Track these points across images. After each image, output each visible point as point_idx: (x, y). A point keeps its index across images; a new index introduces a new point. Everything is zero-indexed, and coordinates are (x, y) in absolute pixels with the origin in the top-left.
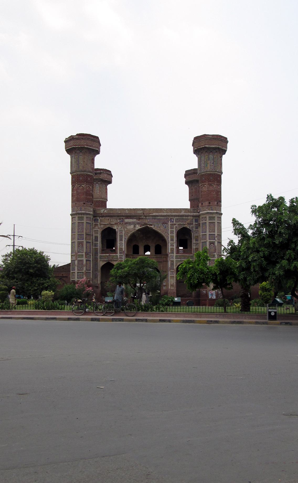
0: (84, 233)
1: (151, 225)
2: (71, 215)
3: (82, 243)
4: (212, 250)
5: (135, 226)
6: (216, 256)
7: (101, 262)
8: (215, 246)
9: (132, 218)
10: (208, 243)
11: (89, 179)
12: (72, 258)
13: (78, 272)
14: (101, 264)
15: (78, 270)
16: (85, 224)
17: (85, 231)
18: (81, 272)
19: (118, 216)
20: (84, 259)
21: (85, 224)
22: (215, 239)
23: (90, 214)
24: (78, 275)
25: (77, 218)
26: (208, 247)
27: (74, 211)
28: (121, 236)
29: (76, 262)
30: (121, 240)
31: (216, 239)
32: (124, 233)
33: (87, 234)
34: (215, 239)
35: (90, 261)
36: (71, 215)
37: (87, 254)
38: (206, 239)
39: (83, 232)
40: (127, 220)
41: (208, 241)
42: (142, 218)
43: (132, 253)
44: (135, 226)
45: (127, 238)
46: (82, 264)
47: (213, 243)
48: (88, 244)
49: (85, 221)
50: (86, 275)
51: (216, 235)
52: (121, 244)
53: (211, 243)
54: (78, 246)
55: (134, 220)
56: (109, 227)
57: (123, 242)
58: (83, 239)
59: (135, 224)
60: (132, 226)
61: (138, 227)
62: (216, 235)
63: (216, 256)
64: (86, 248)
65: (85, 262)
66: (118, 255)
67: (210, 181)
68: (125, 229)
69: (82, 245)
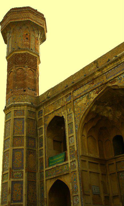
1: (114, 80)
5: (88, 98)
7: (48, 181)
9: (83, 86)
14: (49, 185)
19: (63, 92)
23: (20, 105)
28: (70, 124)
30: (71, 132)
32: (73, 117)
35: (22, 182)
40: (75, 94)
42: (98, 77)
43: (112, 156)
44: (88, 98)
45: (78, 123)
52: (73, 138)
55: (86, 87)
56: (56, 117)
57: (74, 134)
59: (87, 94)
60: (84, 100)
61: (94, 96)
64: (13, 160)
66: (69, 161)
68: (75, 110)
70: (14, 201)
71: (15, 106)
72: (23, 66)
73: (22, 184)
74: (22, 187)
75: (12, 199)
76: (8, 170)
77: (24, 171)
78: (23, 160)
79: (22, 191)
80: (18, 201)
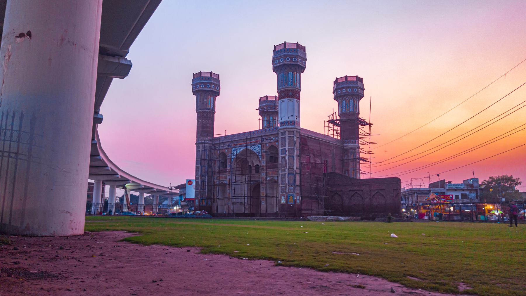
6: (287, 170)
8: (286, 161)
11: (205, 115)
20: (199, 180)
22: (285, 154)
31: (287, 153)
33: (201, 159)
37: (202, 176)
47: (284, 157)
51: (287, 149)
62: (287, 149)
63: (287, 170)
71: (202, 143)
72: (206, 116)
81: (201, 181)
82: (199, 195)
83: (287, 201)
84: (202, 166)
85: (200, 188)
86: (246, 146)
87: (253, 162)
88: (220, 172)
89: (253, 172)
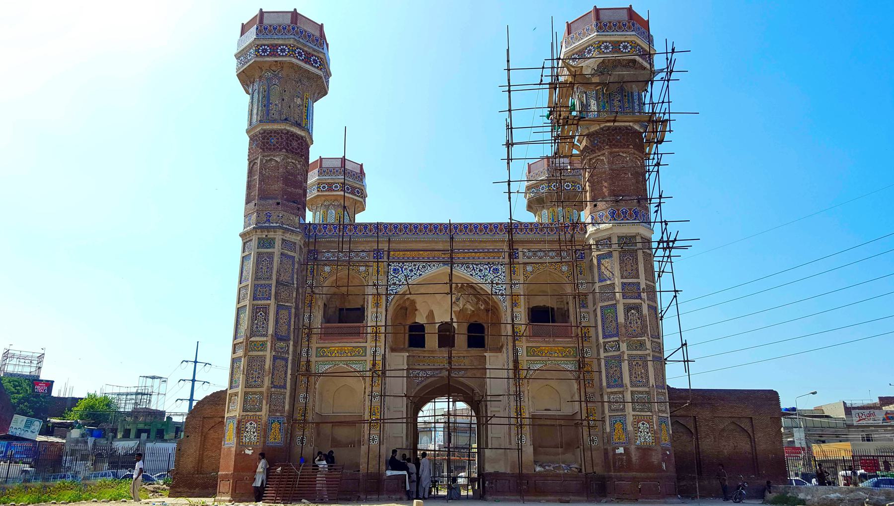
0: (274, 283)
2: (242, 235)
3: (266, 309)
4: (635, 326)
8: (641, 317)
10: (621, 309)
11: (295, 144)
12: (234, 352)
13: (246, 394)
15: (247, 385)
16: (276, 259)
17: (274, 277)
18: (255, 393)
20: (268, 354)
21: (276, 259)
22: (639, 297)
24: (245, 401)
25: (254, 244)
26: (621, 319)
27: (250, 225)
29: (243, 363)
34: (639, 297)
35: (286, 360)
36: (242, 235)
37: (277, 337)
38: (614, 298)
39: (270, 278)
41: (622, 301)
46: (262, 368)
47: (638, 308)
48: (284, 313)
49: (277, 250)
50: (269, 403)
51: (643, 286)
53: (628, 308)
54: (254, 317)
58: (269, 299)
63: (648, 345)
64: (277, 321)
65: (268, 364)
67: (616, 146)
69: (267, 314)
70: (275, 387)
73: (287, 362)
74: (287, 367)
75: (272, 382)
76: (266, 335)
77: (292, 343)
78: (289, 326)
79: (286, 373)
80: (280, 387)
81: (275, 358)
82: (265, 407)
83: (657, 440)
84: (279, 307)
85: (267, 381)
86: (451, 263)
87: (431, 314)
88: (326, 335)
89: (432, 341)
